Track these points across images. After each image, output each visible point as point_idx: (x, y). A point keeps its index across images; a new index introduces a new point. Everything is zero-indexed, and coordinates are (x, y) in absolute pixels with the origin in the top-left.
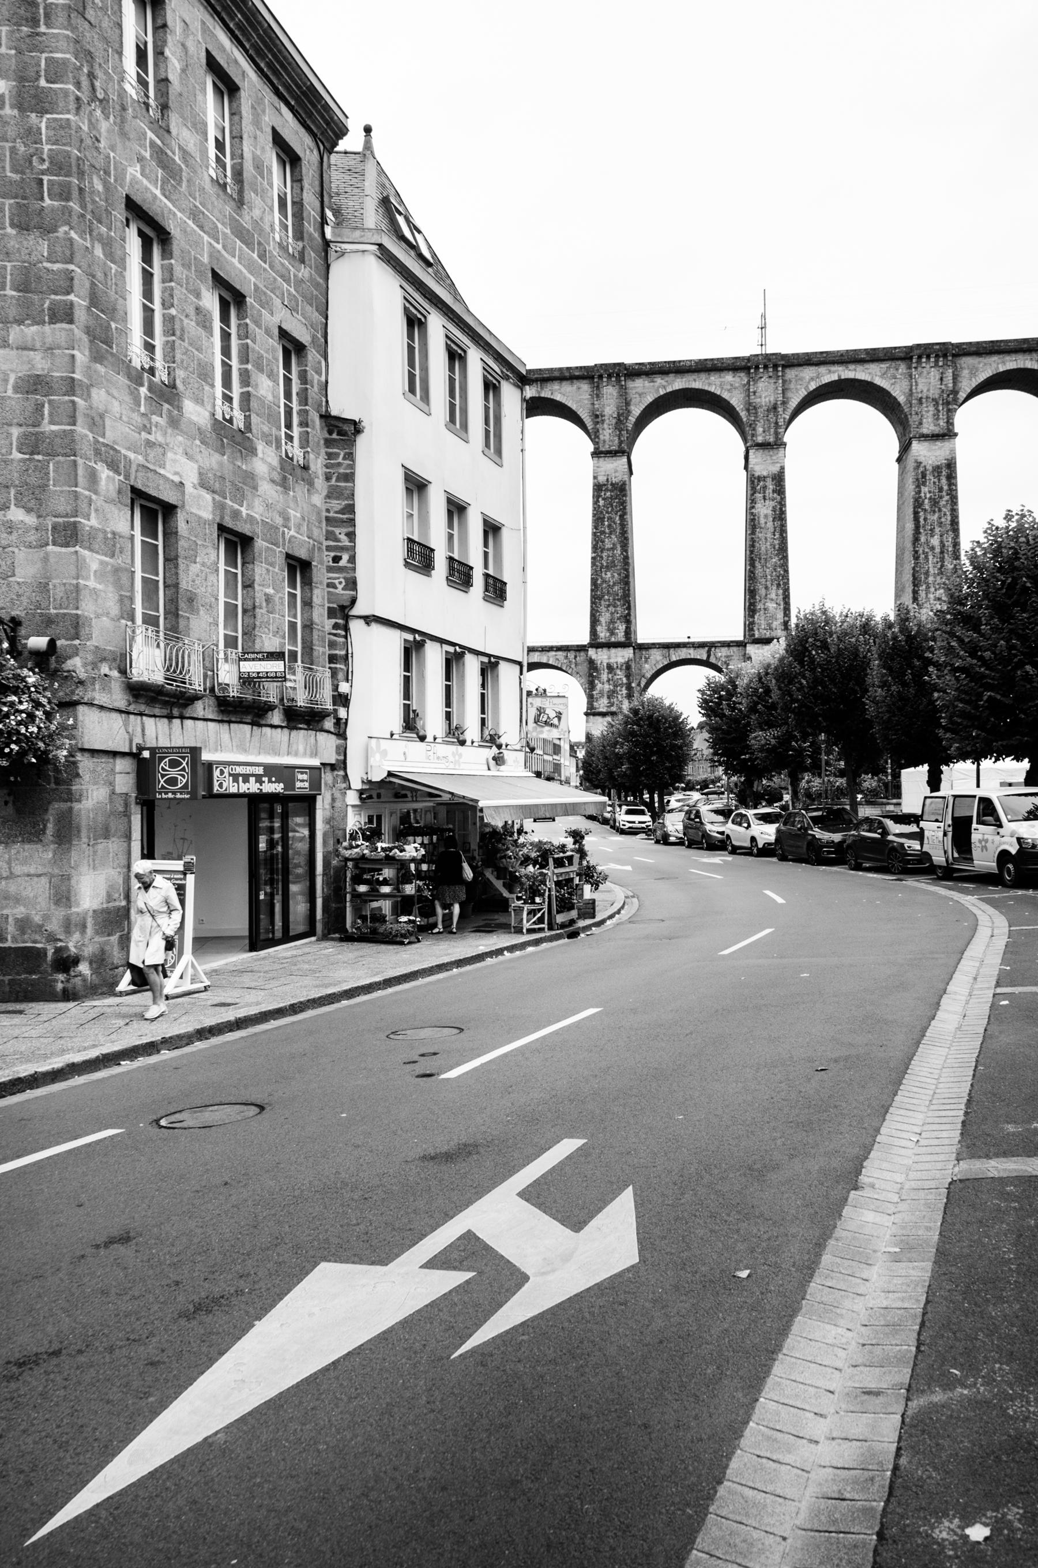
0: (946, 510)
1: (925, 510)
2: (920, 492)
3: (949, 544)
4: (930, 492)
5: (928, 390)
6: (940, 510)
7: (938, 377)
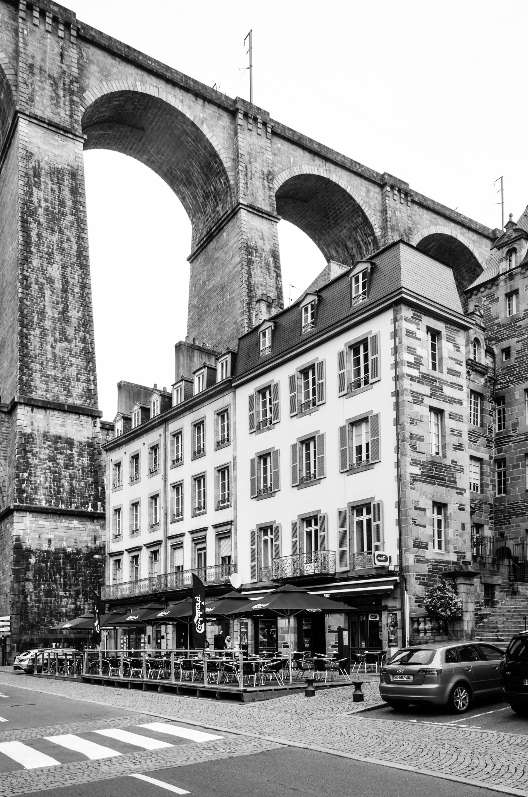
0: (71, 234)
1: (39, 223)
2: (31, 194)
3: (75, 279)
4: (46, 201)
5: (43, 60)
6: (61, 231)
7: (57, 50)
